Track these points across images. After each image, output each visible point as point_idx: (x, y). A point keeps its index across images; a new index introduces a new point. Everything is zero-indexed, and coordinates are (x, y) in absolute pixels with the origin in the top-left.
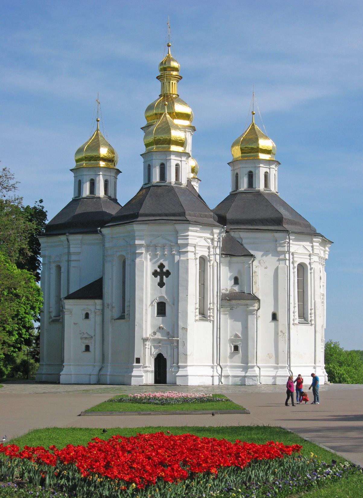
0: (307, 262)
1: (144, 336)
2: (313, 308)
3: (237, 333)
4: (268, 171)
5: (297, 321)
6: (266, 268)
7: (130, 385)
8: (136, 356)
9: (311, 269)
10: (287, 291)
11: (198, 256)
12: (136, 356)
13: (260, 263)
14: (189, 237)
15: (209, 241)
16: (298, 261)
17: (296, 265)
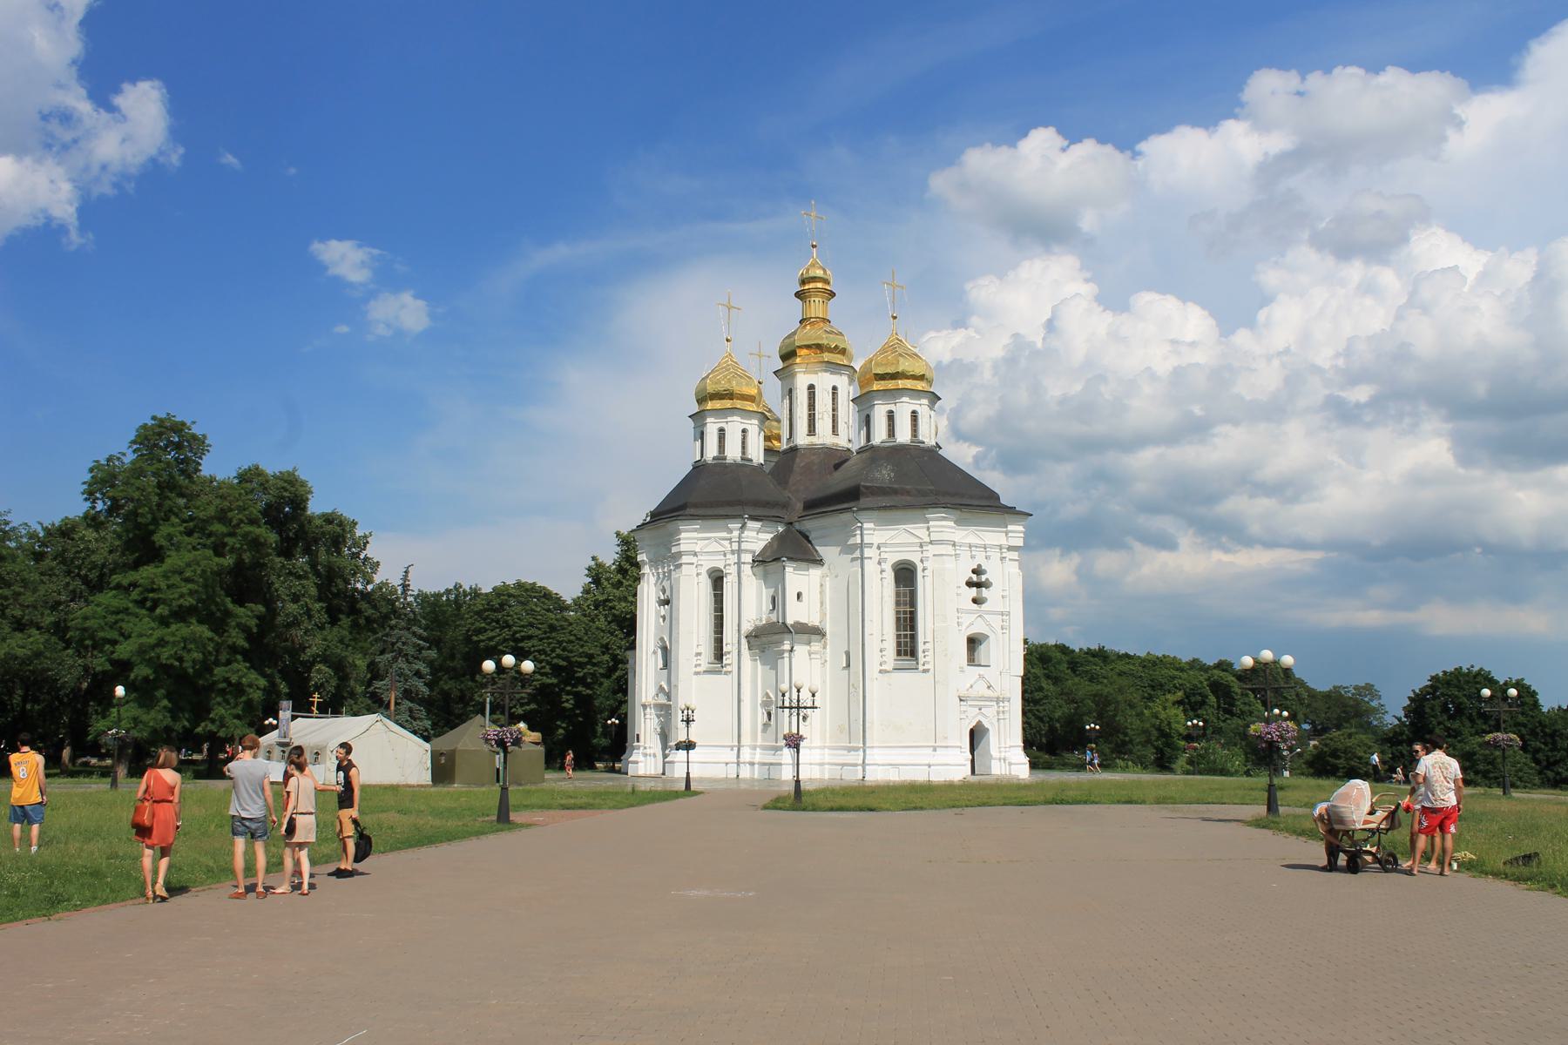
0: (915, 558)
1: (644, 700)
2: (929, 638)
3: (768, 691)
4: (892, 407)
5: (889, 666)
6: (836, 576)
7: (627, 774)
8: (636, 733)
9: (924, 570)
10: (860, 614)
11: (704, 571)
12: (636, 733)
13: (829, 569)
14: (681, 542)
15: (726, 543)
16: (893, 558)
17: (888, 567)
